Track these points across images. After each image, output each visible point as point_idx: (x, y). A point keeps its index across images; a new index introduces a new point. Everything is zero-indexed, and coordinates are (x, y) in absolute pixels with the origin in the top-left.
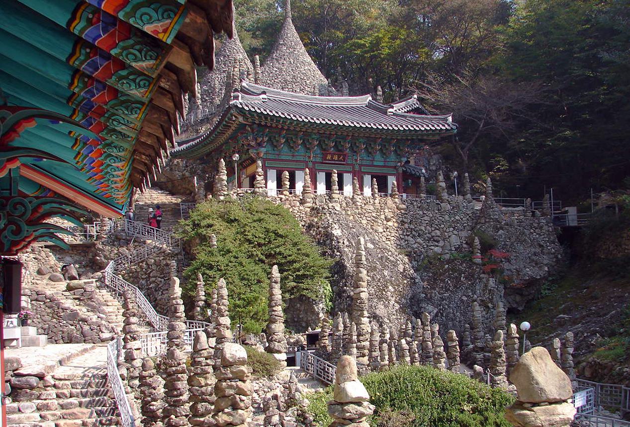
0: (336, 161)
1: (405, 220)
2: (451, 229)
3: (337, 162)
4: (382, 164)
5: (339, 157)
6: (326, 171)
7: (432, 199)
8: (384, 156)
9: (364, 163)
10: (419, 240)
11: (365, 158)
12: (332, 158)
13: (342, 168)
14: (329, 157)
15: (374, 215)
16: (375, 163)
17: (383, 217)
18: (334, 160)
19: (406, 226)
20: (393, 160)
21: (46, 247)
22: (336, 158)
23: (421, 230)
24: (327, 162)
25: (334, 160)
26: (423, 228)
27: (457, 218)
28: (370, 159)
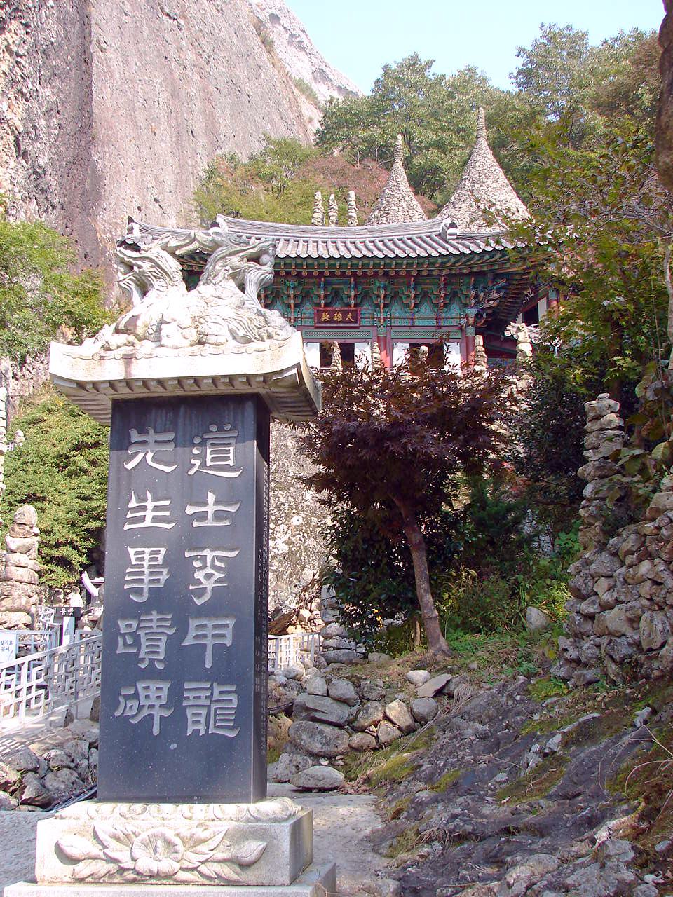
0: (340, 322)
3: (342, 325)
4: (432, 322)
5: (344, 315)
6: (323, 340)
8: (436, 309)
9: (398, 322)
11: (397, 315)
12: (332, 317)
13: (348, 336)
14: (325, 317)
16: (418, 323)
18: (336, 322)
20: (454, 315)
22: (339, 317)
24: (323, 325)
25: (336, 322)
28: (407, 315)
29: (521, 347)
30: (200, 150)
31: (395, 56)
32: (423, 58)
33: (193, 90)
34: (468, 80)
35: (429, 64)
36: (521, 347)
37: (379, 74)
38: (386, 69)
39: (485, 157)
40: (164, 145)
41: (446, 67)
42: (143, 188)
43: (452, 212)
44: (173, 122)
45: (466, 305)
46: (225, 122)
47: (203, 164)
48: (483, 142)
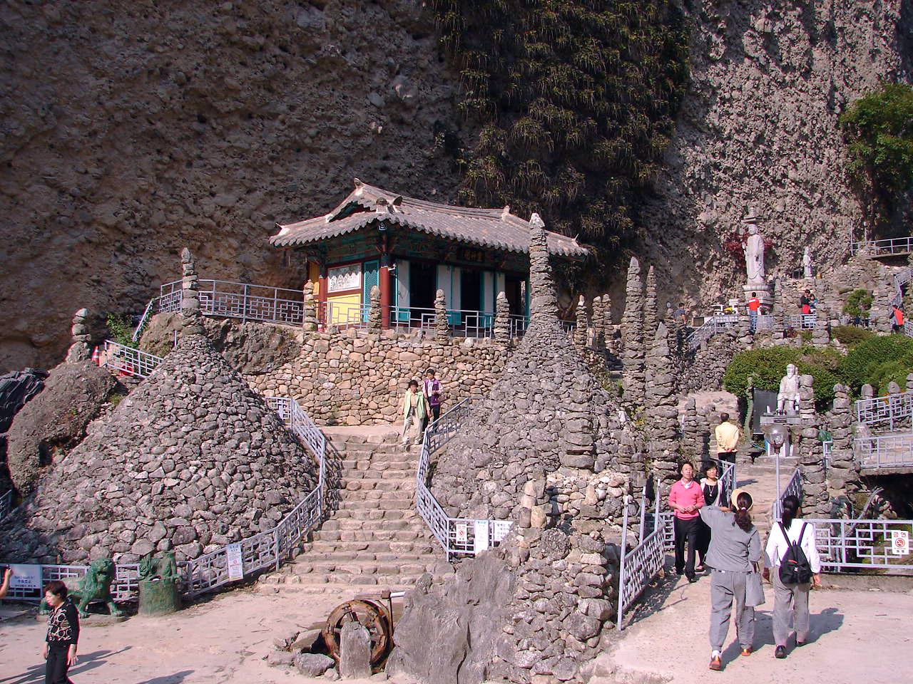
21: (874, 259)
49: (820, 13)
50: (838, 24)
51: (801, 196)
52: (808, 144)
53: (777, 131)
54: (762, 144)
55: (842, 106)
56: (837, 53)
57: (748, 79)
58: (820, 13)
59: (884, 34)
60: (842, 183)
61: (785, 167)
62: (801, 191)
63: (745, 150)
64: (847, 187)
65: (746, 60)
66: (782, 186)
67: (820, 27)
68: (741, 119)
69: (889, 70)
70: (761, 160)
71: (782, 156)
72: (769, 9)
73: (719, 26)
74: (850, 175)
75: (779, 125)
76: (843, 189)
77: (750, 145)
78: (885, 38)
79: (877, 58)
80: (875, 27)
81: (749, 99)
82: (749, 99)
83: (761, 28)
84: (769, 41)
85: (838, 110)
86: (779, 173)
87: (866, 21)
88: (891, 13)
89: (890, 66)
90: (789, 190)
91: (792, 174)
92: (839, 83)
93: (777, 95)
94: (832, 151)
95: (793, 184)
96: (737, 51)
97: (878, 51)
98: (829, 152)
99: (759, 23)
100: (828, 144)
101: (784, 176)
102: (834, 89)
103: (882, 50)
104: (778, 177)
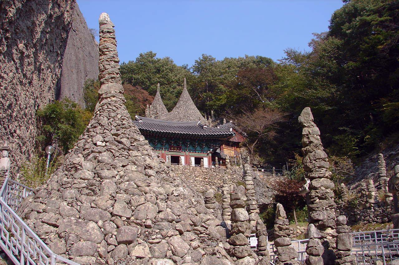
1: (206, 177)
2: (231, 182)
7: (223, 167)
10: (213, 187)
15: (189, 174)
17: (193, 175)
19: (207, 180)
23: (215, 182)
26: (216, 181)
27: (234, 177)
29: (227, 160)
30: (82, 77)
31: (144, 51)
32: (154, 52)
33: (80, 56)
34: (167, 61)
35: (155, 55)
36: (227, 160)
37: (138, 56)
38: (141, 55)
39: (186, 94)
40: (75, 76)
41: (160, 56)
42: (70, 90)
43: (178, 110)
44: (76, 68)
45: (209, 148)
46: (88, 67)
47: (83, 83)
48: (185, 88)
49: (39, 57)
50: (42, 67)
51: (20, 146)
52: (26, 119)
53: (17, 106)
54: (10, 109)
55: (38, 106)
56: (40, 80)
57: (11, 71)
58: (39, 57)
59: (54, 82)
60: (33, 145)
61: (16, 126)
62: (20, 143)
63: (3, 109)
64: (34, 149)
65: (13, 62)
66: (13, 136)
67: (38, 64)
68: (5, 91)
69: (53, 99)
70: (8, 118)
71: (16, 120)
72: (26, 42)
73: (8, 35)
74: (36, 141)
75: (18, 102)
76: (33, 149)
77: (6, 107)
78: (53, 83)
79: (50, 92)
80: (52, 76)
81: (10, 82)
82: (10, 82)
83: (21, 48)
84: (22, 56)
85: (36, 108)
86: (14, 129)
87: (50, 72)
88: (58, 73)
89: (53, 98)
90: (15, 140)
91: (18, 132)
92: (39, 96)
93: (19, 87)
94: (33, 127)
95: (18, 137)
96: (9, 55)
97: (51, 87)
98: (31, 127)
99: (21, 46)
100: (32, 123)
101: (15, 132)
102: (37, 98)
103: (52, 88)
104: (13, 131)
